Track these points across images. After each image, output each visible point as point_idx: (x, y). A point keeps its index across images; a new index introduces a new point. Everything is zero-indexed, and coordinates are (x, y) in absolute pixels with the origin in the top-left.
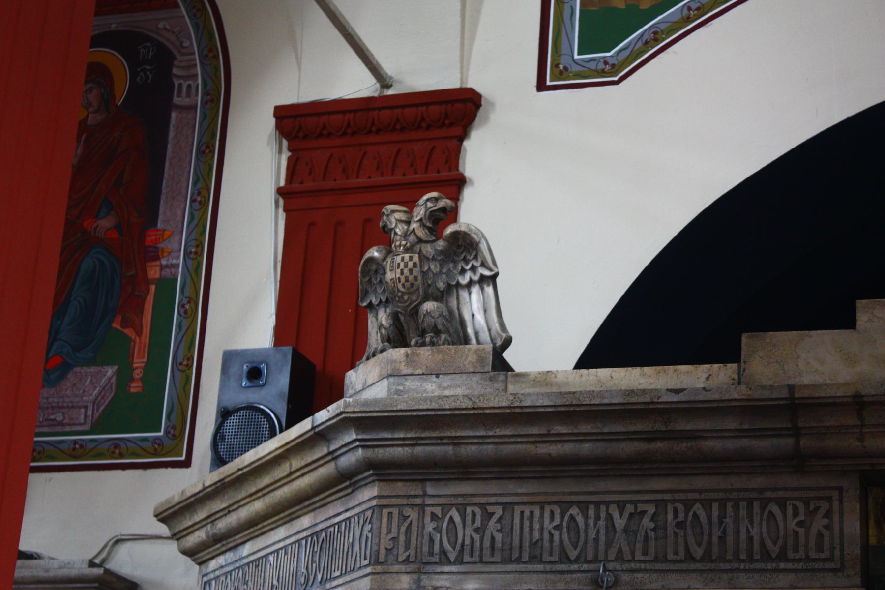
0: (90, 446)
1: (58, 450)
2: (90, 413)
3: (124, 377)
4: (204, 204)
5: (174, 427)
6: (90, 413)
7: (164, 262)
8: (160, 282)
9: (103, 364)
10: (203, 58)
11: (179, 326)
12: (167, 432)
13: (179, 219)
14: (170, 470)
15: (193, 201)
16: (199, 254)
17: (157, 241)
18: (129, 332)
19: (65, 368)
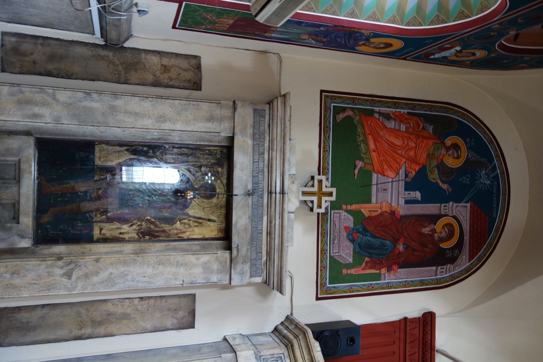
0: (325, 257)
1: (324, 243)
2: (337, 254)
3: (349, 266)
4: (405, 286)
5: (330, 290)
6: (337, 254)
7: (386, 274)
8: (380, 274)
9: (353, 256)
10: (451, 276)
11: (364, 285)
12: (328, 288)
13: (400, 277)
14: (315, 292)
15: (406, 282)
16: (388, 287)
17: (394, 270)
18: (364, 265)
19: (353, 241)
